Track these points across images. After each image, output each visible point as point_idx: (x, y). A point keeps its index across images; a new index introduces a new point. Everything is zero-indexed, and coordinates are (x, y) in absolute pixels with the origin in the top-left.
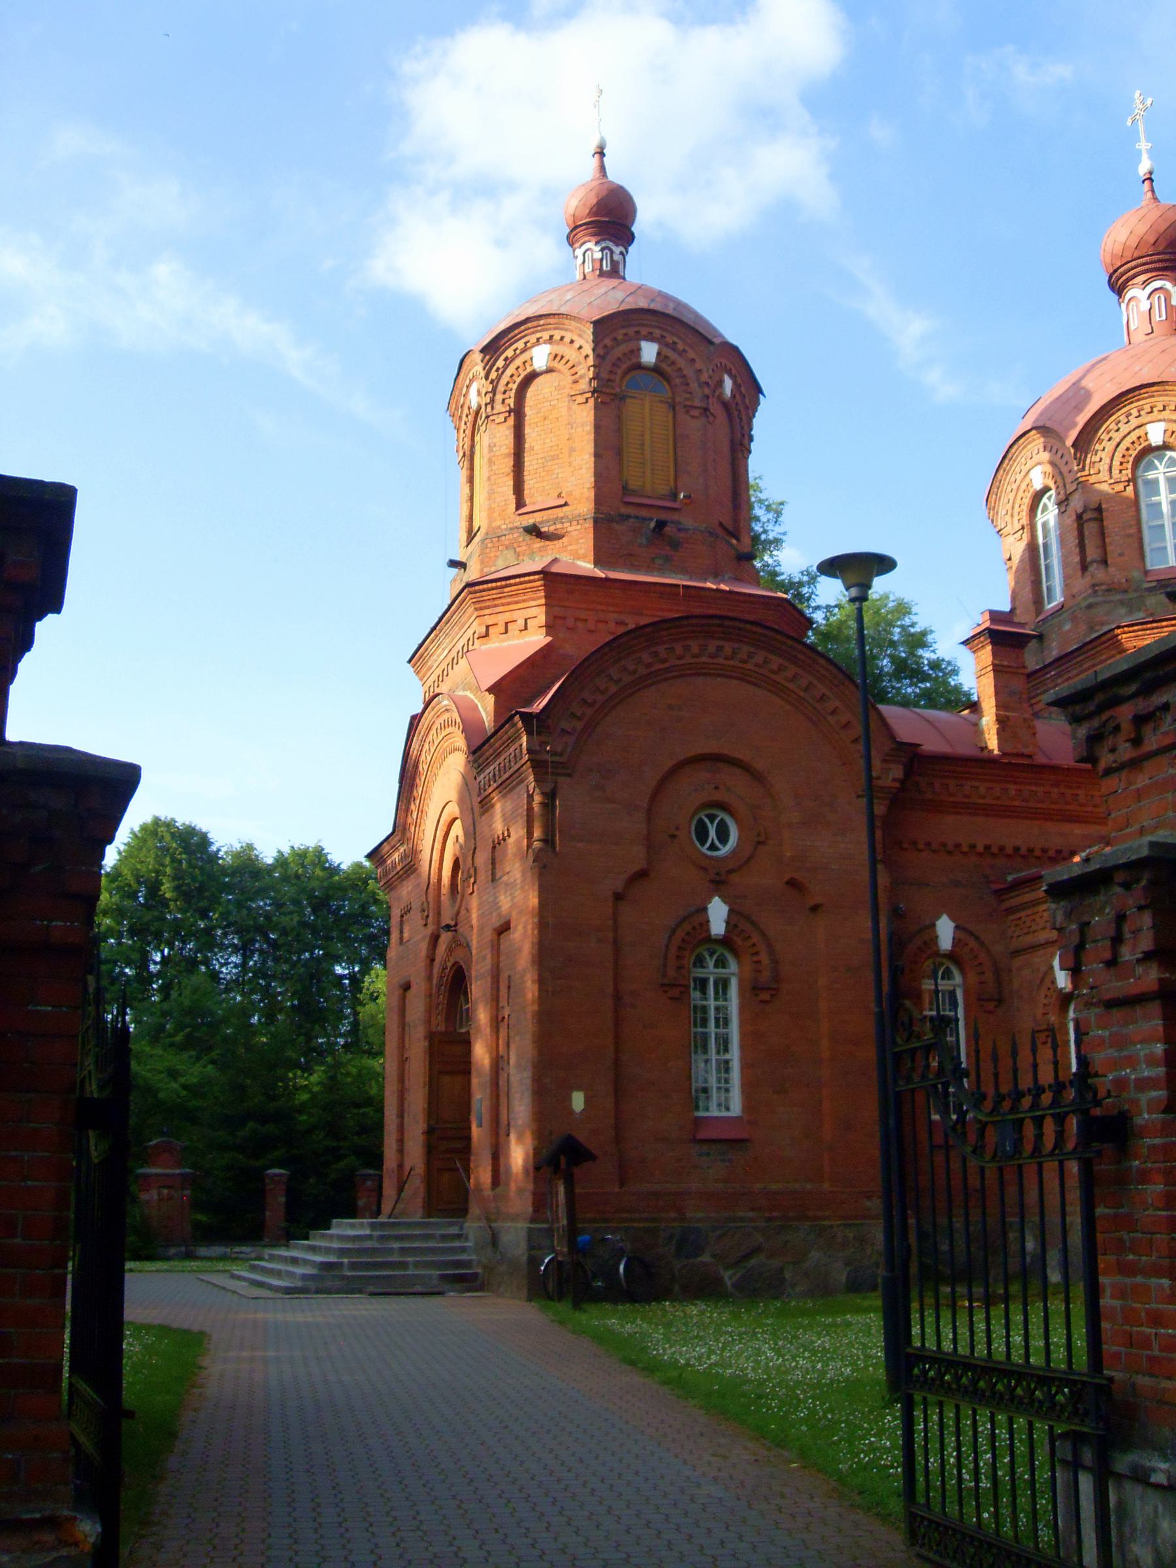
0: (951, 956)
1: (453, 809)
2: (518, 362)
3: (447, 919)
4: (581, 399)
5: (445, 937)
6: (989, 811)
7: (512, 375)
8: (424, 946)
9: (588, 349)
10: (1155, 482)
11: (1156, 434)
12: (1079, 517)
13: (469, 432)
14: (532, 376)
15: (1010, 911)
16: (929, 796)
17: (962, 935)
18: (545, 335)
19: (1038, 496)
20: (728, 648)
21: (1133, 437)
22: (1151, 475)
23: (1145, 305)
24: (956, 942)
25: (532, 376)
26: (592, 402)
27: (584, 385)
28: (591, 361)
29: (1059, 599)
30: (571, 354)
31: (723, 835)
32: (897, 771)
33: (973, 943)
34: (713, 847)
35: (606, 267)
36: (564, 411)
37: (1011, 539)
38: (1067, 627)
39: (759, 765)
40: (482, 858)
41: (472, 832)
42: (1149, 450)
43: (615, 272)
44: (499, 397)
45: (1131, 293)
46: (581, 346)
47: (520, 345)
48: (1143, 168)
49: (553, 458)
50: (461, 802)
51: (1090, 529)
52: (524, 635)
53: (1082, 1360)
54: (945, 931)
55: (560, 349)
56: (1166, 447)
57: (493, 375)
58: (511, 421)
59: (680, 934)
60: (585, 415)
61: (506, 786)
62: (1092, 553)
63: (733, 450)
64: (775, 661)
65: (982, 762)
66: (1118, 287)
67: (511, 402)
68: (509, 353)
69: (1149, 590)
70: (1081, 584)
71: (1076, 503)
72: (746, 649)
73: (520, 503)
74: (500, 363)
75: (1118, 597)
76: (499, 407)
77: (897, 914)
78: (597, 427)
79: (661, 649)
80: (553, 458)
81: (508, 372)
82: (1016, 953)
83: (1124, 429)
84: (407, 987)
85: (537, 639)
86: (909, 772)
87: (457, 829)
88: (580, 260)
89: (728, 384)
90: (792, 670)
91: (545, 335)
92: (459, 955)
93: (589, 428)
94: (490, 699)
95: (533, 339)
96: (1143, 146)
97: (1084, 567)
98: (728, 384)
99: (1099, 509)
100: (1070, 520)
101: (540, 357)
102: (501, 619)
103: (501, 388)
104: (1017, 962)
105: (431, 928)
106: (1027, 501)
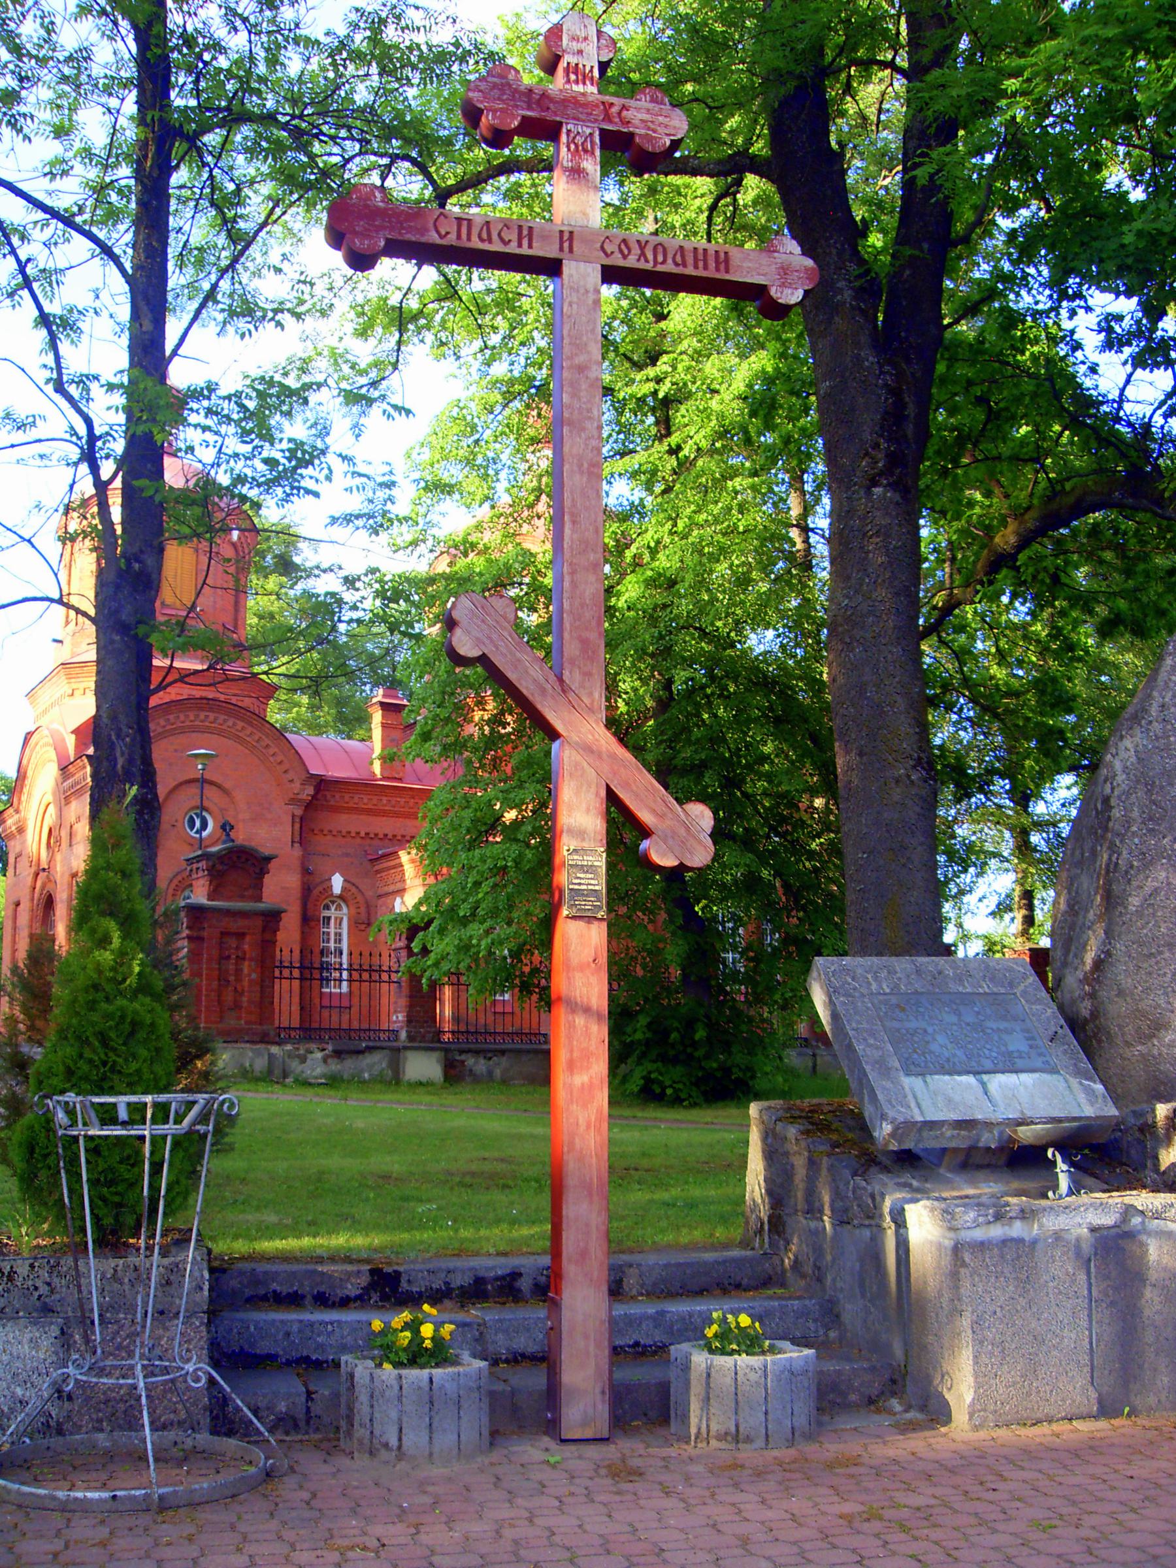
0: (341, 897)
1: (49, 798)
3: (44, 865)
5: (42, 875)
6: (369, 812)
8: (30, 879)
15: (378, 872)
16: (332, 803)
17: (348, 885)
20: (212, 716)
24: (344, 889)
31: (204, 825)
32: (310, 790)
33: (354, 890)
39: (228, 785)
40: (64, 834)
41: (60, 815)
50: (54, 794)
54: (337, 883)
59: (175, 882)
61: (78, 793)
64: (240, 724)
65: (366, 786)
72: (222, 717)
77: (306, 872)
79: (171, 717)
82: (380, 896)
84: (18, 904)
86: (318, 789)
87: (52, 810)
90: (249, 730)
92: (49, 887)
94: (73, 737)
102: (82, 686)
104: (381, 902)
105: (33, 870)
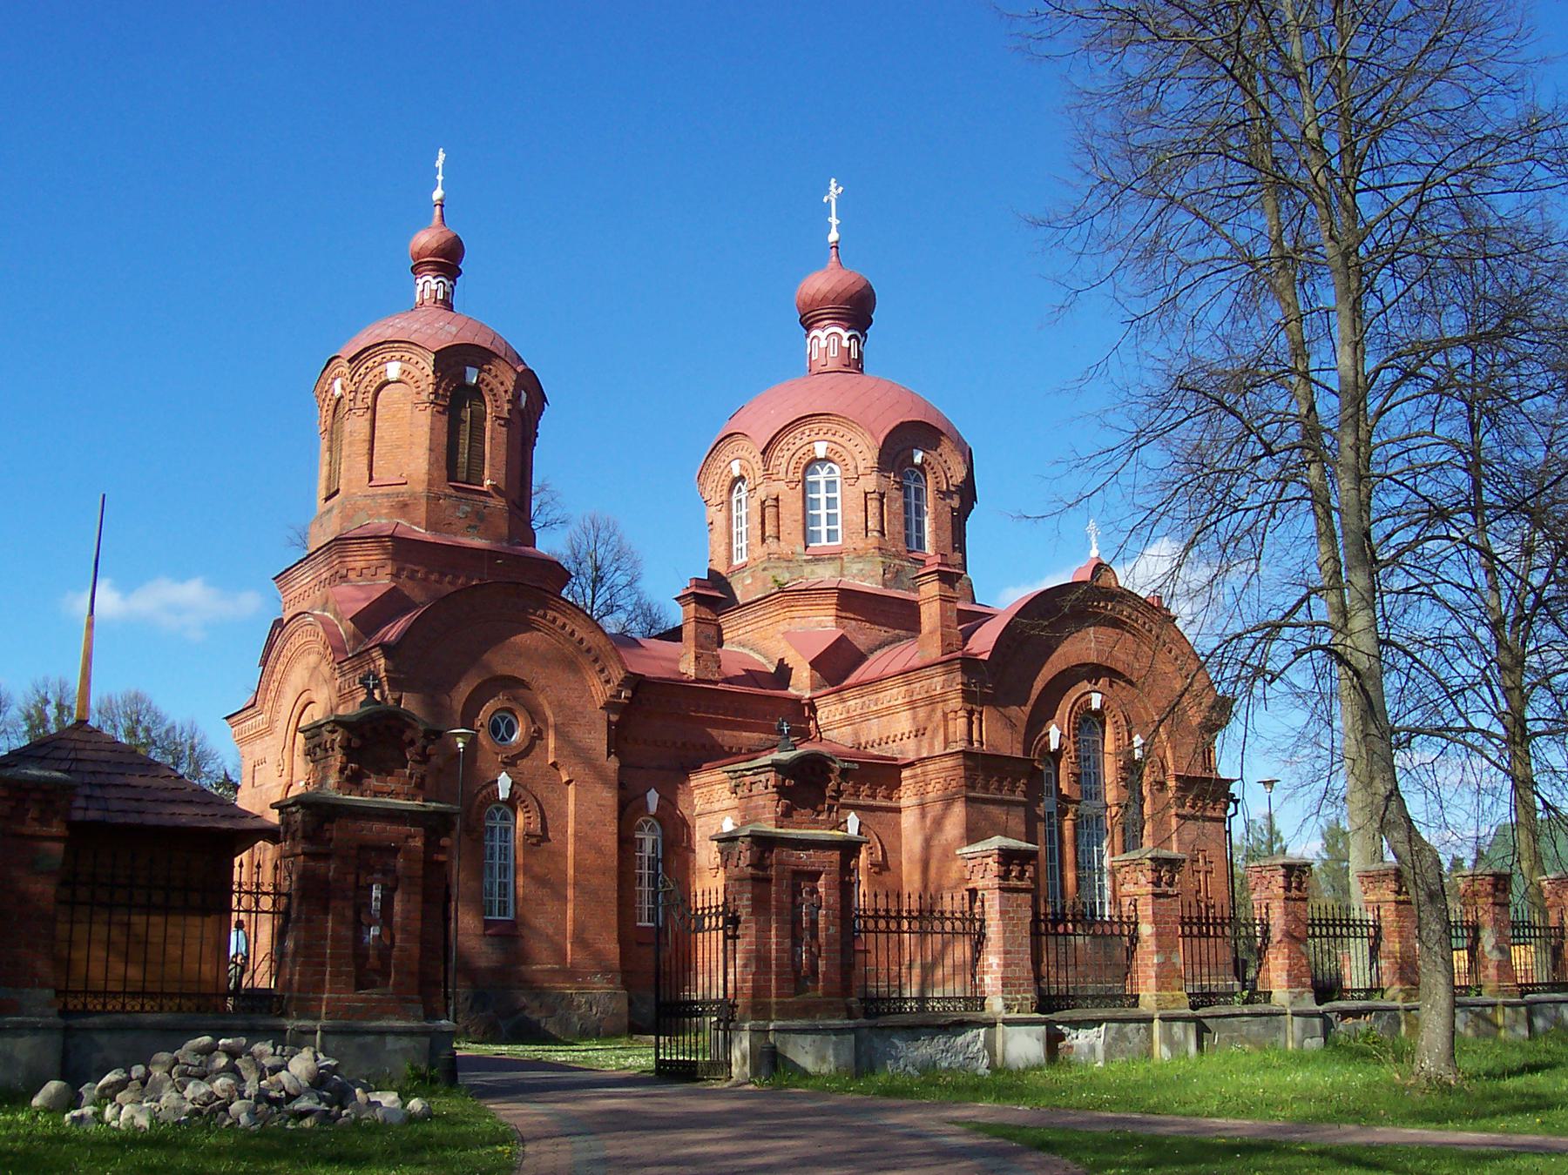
2: (376, 371)
4: (422, 407)
7: (370, 381)
9: (429, 370)
10: (817, 483)
11: (821, 450)
12: (763, 503)
13: (331, 413)
14: (388, 383)
18: (398, 355)
19: (735, 481)
21: (805, 449)
22: (810, 478)
23: (823, 344)
25: (388, 383)
26: (429, 411)
27: (424, 397)
28: (431, 379)
29: (745, 559)
30: (417, 374)
34: (503, 739)
35: (440, 296)
36: (408, 413)
37: (713, 509)
38: (749, 581)
42: (815, 460)
43: (447, 304)
44: (360, 396)
45: (814, 333)
46: (425, 367)
47: (378, 359)
48: (833, 236)
49: (399, 447)
51: (770, 512)
52: (372, 579)
53: (721, 996)
55: (406, 366)
56: (827, 460)
57: (356, 379)
58: (368, 415)
60: (424, 418)
62: (770, 530)
63: (523, 444)
66: (808, 324)
67: (369, 401)
68: (370, 364)
69: (806, 561)
70: (760, 551)
71: (761, 493)
73: (371, 479)
74: (362, 370)
75: (785, 564)
76: (359, 404)
78: (432, 429)
80: (399, 447)
81: (368, 378)
83: (799, 443)
85: (384, 582)
88: (420, 288)
89: (524, 395)
91: (398, 355)
93: (427, 429)
95: (388, 356)
96: (834, 220)
97: (763, 540)
98: (524, 395)
99: (777, 499)
100: (756, 504)
101: (393, 370)
103: (362, 389)
106: (727, 483)
